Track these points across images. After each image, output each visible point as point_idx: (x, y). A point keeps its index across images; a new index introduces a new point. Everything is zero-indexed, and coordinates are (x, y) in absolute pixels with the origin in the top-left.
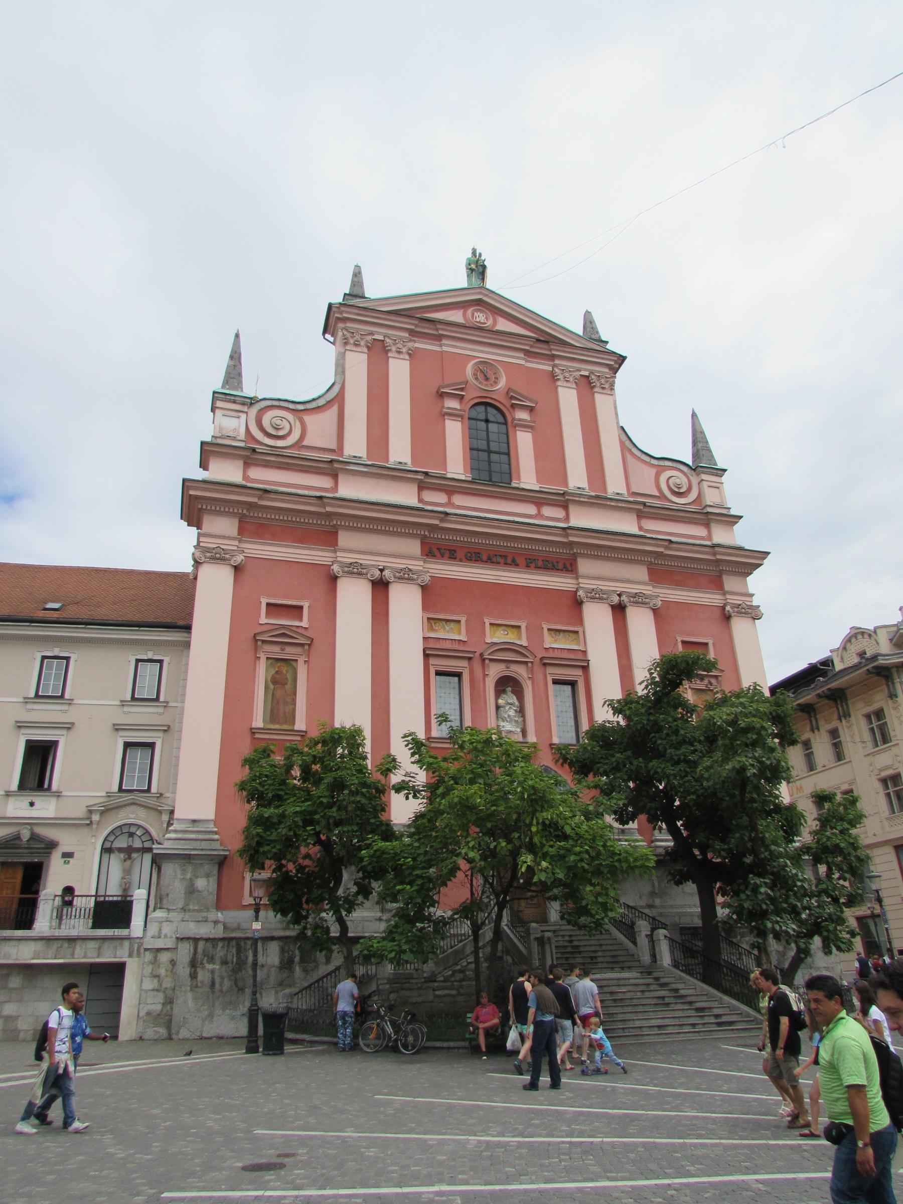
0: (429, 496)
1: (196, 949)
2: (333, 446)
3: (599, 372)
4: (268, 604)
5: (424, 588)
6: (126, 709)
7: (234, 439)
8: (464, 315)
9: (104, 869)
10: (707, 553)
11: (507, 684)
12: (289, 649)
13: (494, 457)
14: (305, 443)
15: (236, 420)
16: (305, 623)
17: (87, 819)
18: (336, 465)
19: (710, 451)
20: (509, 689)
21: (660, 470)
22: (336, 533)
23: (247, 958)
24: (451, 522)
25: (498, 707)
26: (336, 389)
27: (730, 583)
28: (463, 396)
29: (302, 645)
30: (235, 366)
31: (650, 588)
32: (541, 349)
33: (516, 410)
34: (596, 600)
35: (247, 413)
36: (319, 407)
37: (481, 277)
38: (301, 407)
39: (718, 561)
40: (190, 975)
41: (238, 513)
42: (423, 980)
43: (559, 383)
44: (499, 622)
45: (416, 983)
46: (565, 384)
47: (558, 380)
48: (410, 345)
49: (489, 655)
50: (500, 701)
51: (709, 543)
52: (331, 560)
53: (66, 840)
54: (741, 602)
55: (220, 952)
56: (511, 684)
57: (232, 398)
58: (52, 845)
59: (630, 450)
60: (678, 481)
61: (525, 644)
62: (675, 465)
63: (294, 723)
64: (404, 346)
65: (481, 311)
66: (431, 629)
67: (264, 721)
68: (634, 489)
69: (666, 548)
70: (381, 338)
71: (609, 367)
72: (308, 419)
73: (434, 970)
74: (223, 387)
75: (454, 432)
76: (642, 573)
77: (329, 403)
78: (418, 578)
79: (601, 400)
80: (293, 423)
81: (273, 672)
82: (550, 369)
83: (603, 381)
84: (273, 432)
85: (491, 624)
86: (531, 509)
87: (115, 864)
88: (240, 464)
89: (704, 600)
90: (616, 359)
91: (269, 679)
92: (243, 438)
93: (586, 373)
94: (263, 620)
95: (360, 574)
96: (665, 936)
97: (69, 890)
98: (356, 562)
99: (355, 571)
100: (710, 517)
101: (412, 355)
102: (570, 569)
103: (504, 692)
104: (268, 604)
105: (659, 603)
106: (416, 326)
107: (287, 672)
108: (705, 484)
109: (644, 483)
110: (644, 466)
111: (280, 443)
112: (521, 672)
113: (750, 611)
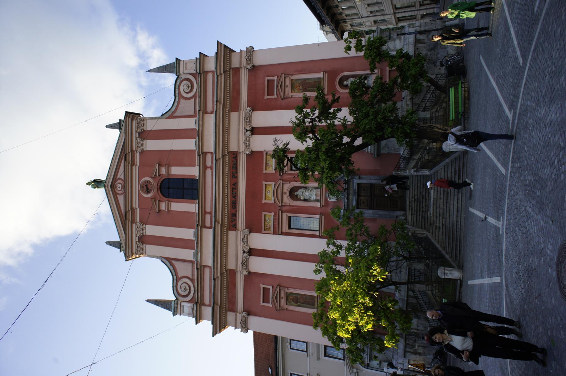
0: (208, 224)
1: (409, 352)
2: (190, 264)
3: (136, 128)
4: (263, 302)
5: (250, 232)
6: (311, 355)
7: (193, 309)
8: (120, 194)
9: (376, 369)
10: (221, 79)
12: (282, 295)
13: (185, 186)
15: (184, 307)
16: (271, 287)
17: (355, 374)
18: (199, 267)
19: (167, 65)
20: (296, 193)
21: (181, 96)
22: (230, 270)
23: (413, 332)
24: (219, 218)
25: (305, 200)
26: (165, 260)
27: (235, 63)
28: (158, 201)
29: (280, 290)
30: (161, 305)
31: (241, 112)
32: (129, 157)
33: (161, 173)
34: (250, 144)
35: (181, 302)
36: (174, 269)
37: (100, 183)
38: (175, 277)
39: (224, 72)
40: (419, 355)
41: (226, 232)
42: (428, 270)
43: (145, 150)
44: (264, 195)
45: (429, 273)
46: (144, 146)
47: (143, 150)
48: (138, 224)
49: (280, 203)
50: (302, 198)
51: (215, 74)
52: (244, 154)
54: (245, 59)
55: (411, 342)
56: (293, 193)
57: (175, 308)
59: (173, 112)
60: (185, 87)
61: (273, 183)
62: (177, 87)
63: (314, 296)
64: (139, 227)
65: (116, 186)
66: (269, 228)
67: (314, 308)
68: (192, 113)
69: (220, 103)
70: (137, 238)
71: (132, 120)
72: (180, 275)
73: (423, 264)
74: (171, 311)
75: (177, 206)
76: (234, 116)
77: (172, 264)
78: (246, 235)
79: (150, 126)
80: (183, 282)
81: (293, 302)
82: (138, 154)
83: (140, 125)
84: (187, 291)
85: (265, 200)
86: (209, 171)
88: (203, 307)
89: (243, 175)
90: (127, 117)
91: (295, 304)
93: (137, 134)
94: (270, 305)
95: (247, 262)
96: (415, 171)
98: (242, 263)
99: (245, 263)
100: (202, 72)
101: (143, 222)
102: (235, 155)
103: (297, 196)
104: (263, 302)
105: (249, 109)
106: (129, 221)
107: (292, 296)
108: (186, 72)
109: (188, 106)
110: (180, 105)
111: (192, 288)
112: (287, 187)
113: (249, 53)
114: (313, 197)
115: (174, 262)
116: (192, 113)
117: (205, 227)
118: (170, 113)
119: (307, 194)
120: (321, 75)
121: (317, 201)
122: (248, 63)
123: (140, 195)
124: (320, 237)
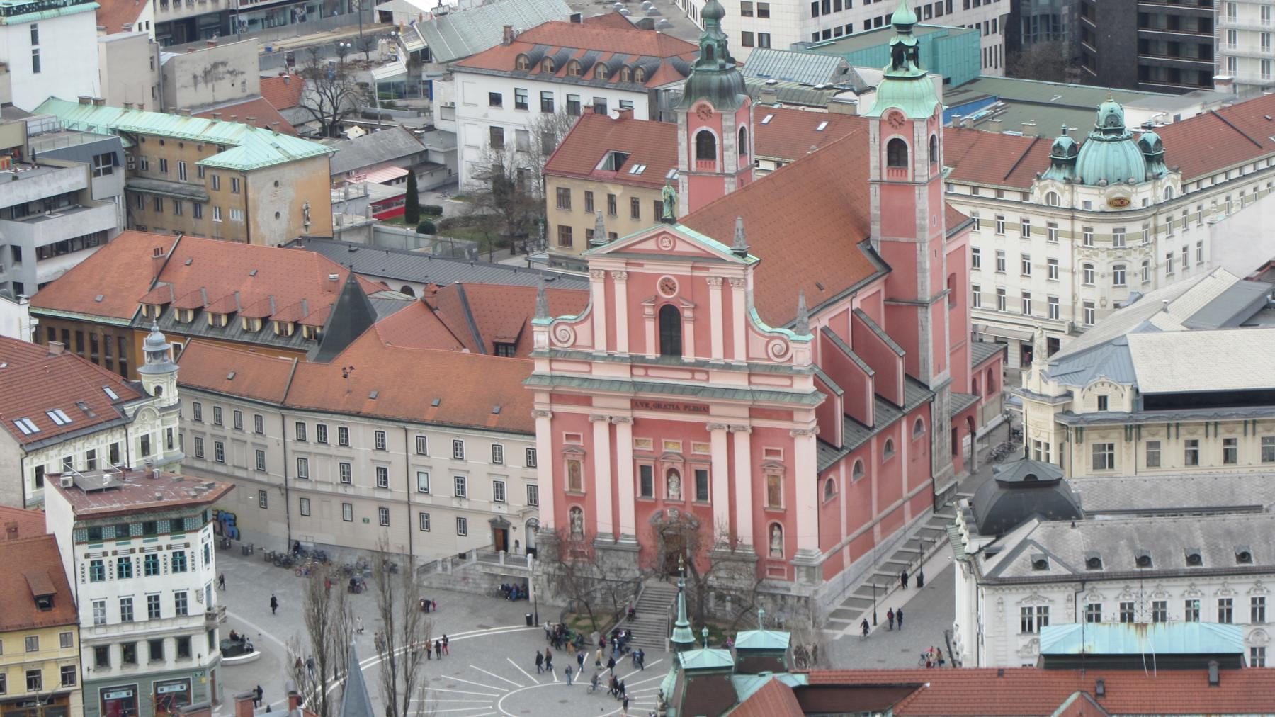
0: (636, 371)
11: (672, 472)
14: (577, 344)
16: (581, 443)
25: (668, 484)
53: (514, 522)
58: (508, 524)
60: (777, 348)
75: (651, 329)
77: (587, 317)
86: (689, 375)
87: (531, 531)
88: (547, 362)
92: (547, 346)
97: (517, 542)
109: (758, 351)
111: (566, 345)
112: (679, 467)
114: (671, 492)
115: (589, 320)
116: (751, 355)
117: (632, 367)
118: (752, 323)
119: (673, 486)
120: (783, 506)
121: (668, 495)
122: (795, 431)
123: (661, 275)
124: (636, 499)
